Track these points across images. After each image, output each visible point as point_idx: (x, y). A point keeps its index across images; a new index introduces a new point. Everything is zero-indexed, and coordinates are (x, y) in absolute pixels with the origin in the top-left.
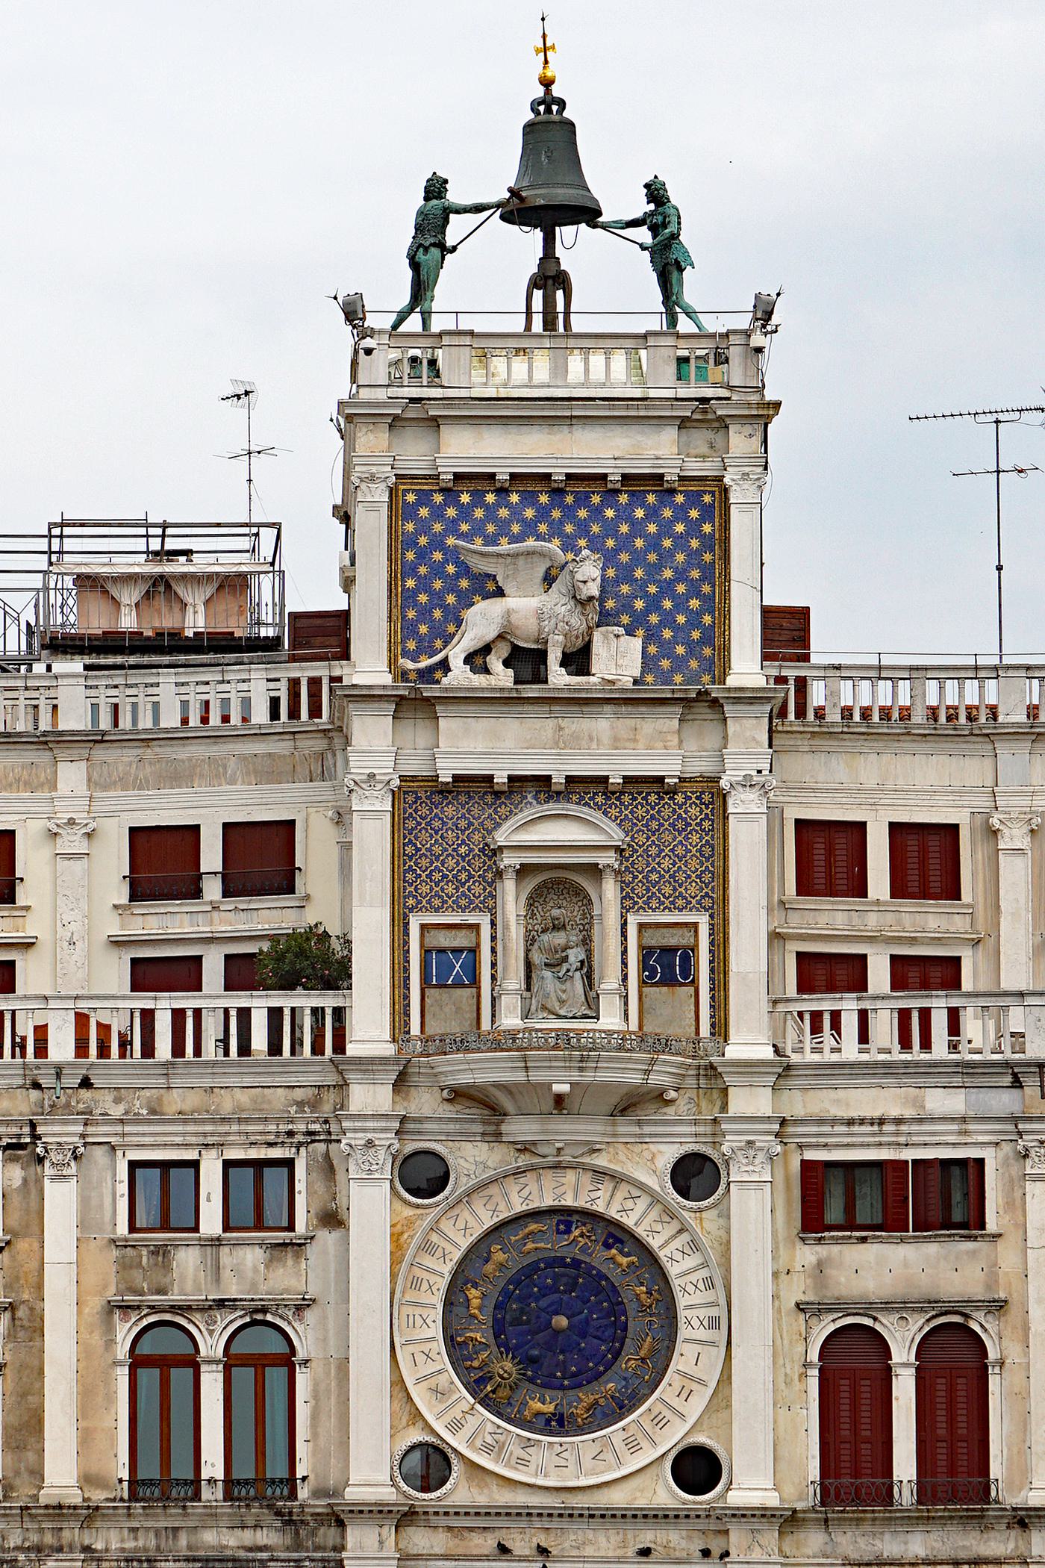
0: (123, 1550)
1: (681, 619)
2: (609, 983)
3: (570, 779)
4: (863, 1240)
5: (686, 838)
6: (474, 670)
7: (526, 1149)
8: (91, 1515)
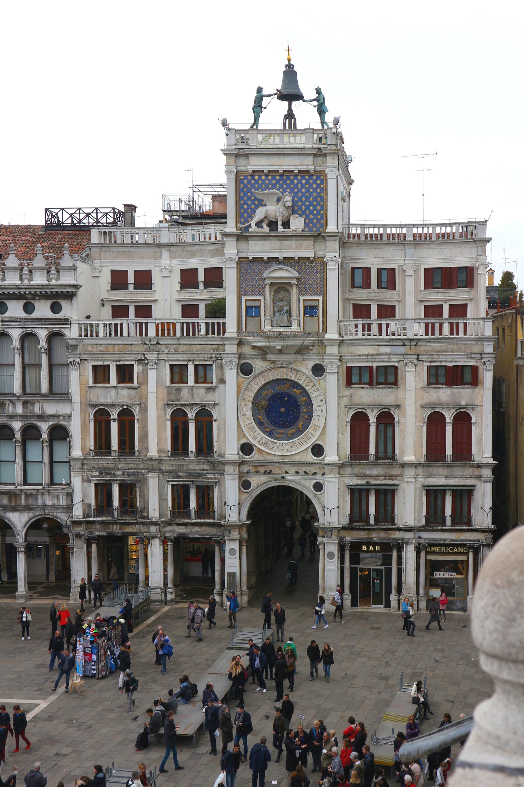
0: (169, 470)
1: (315, 212)
2: (294, 317)
3: (284, 258)
4: (363, 388)
6: (258, 227)
7: (273, 362)
8: (160, 461)
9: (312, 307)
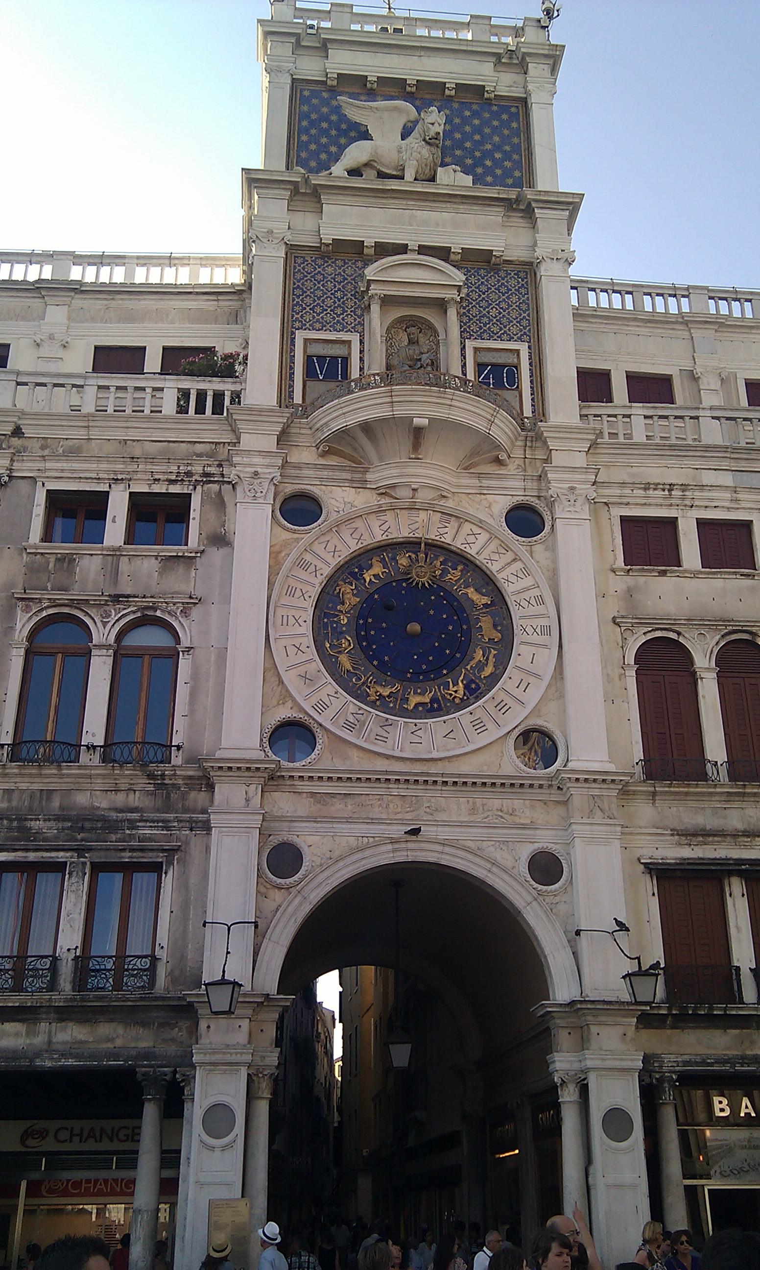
7: (385, 492)
9: (497, 368)
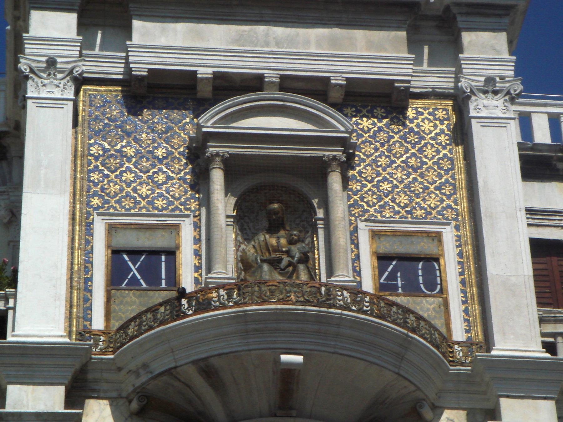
5: (421, 150)
